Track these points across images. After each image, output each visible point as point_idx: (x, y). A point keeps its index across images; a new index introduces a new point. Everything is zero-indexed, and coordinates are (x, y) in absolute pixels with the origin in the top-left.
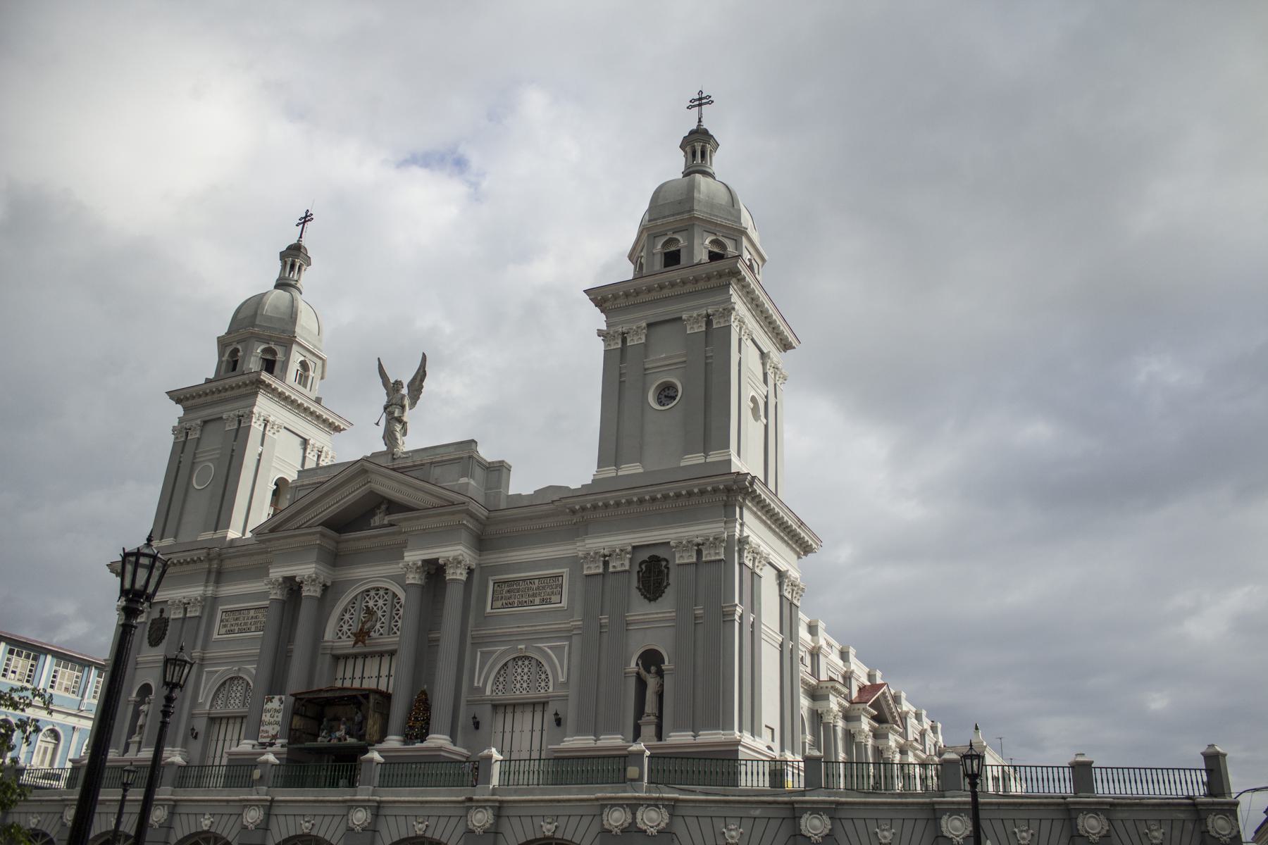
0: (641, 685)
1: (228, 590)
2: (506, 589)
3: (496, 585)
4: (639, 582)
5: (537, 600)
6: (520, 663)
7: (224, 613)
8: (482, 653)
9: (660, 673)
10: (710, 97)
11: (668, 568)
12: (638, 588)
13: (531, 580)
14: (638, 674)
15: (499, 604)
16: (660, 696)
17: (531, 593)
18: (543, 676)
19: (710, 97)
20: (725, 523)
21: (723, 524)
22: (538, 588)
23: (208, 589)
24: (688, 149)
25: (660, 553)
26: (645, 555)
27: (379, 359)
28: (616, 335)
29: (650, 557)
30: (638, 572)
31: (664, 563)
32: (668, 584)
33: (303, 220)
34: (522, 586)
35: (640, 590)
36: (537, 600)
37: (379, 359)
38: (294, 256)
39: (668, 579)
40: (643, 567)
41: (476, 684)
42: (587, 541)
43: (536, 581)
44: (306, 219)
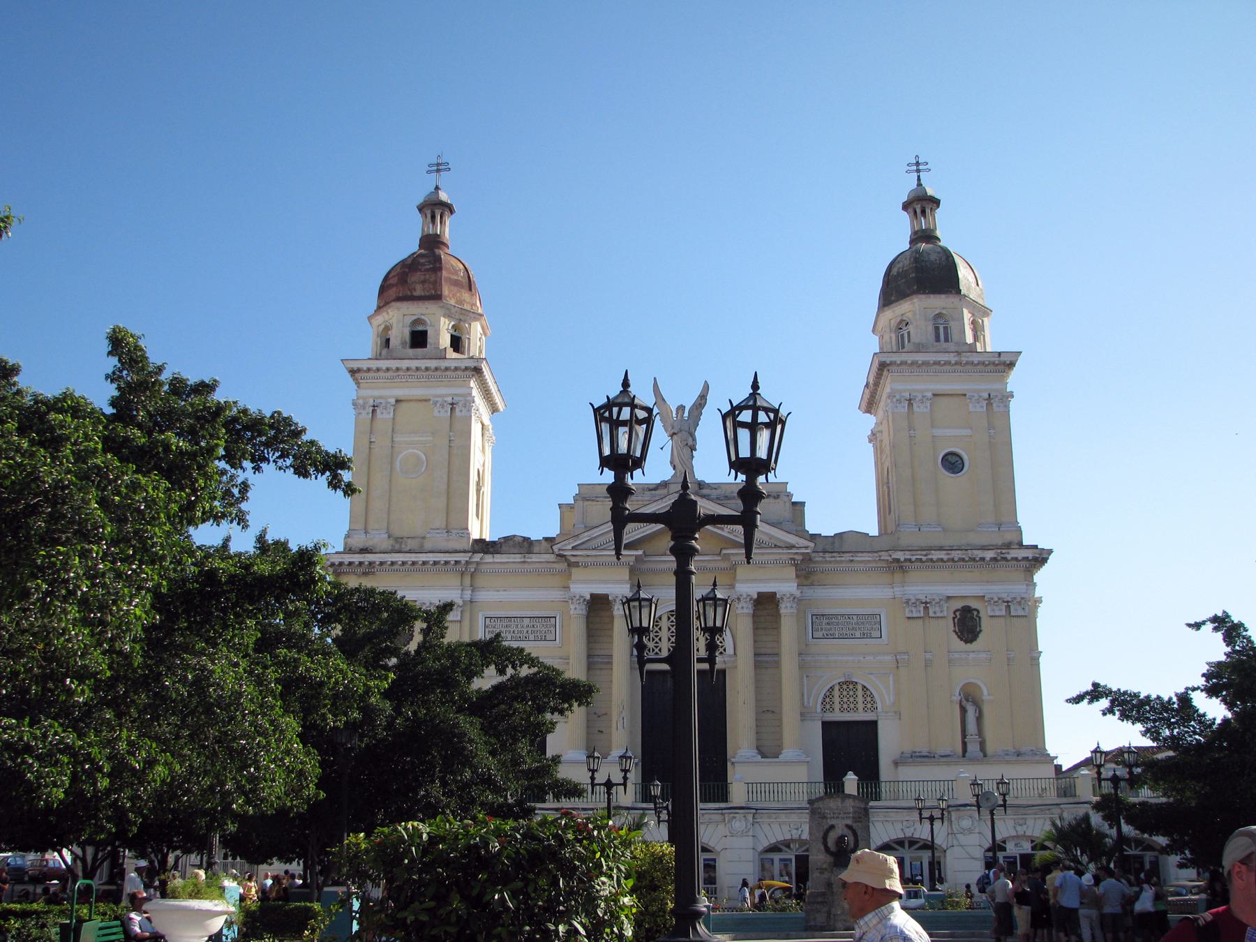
0: (963, 711)
1: (482, 596)
2: (825, 621)
3: (814, 617)
4: (955, 626)
5: (858, 634)
6: (845, 687)
7: (488, 620)
8: (807, 676)
9: (978, 704)
10: (927, 164)
11: (980, 618)
12: (955, 631)
13: (850, 616)
14: (961, 701)
15: (819, 634)
16: (979, 719)
17: (851, 627)
18: (869, 699)
19: (927, 164)
20: (1027, 585)
21: (1025, 587)
22: (858, 623)
23: (465, 592)
24: (911, 210)
25: (974, 604)
26: (959, 605)
27: (655, 379)
28: (902, 400)
29: (963, 607)
30: (954, 619)
31: (975, 613)
32: (981, 631)
33: (435, 168)
34: (842, 620)
35: (956, 633)
36: (858, 634)
37: (655, 379)
38: (434, 208)
39: (980, 626)
40: (958, 614)
41: (806, 703)
42: (906, 588)
43: (855, 617)
44: (439, 168)
